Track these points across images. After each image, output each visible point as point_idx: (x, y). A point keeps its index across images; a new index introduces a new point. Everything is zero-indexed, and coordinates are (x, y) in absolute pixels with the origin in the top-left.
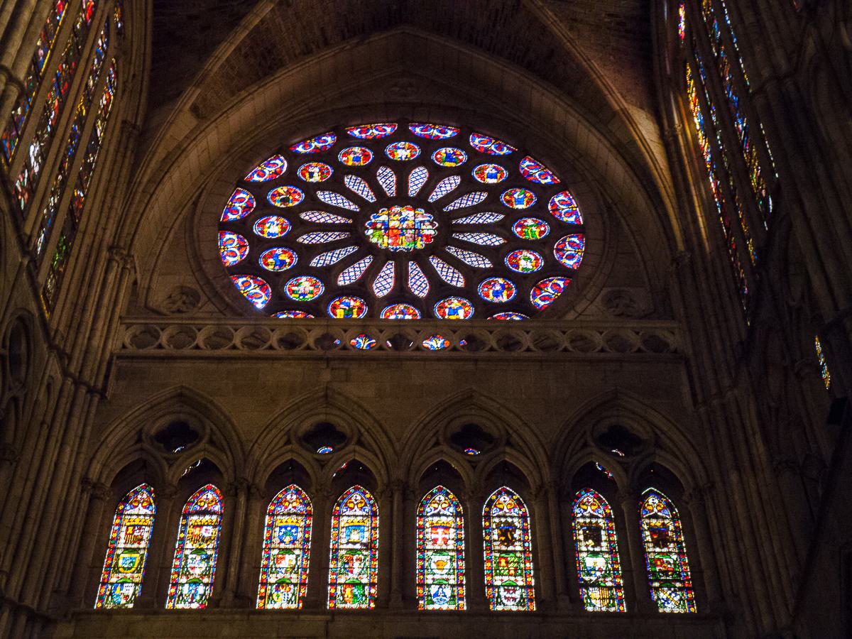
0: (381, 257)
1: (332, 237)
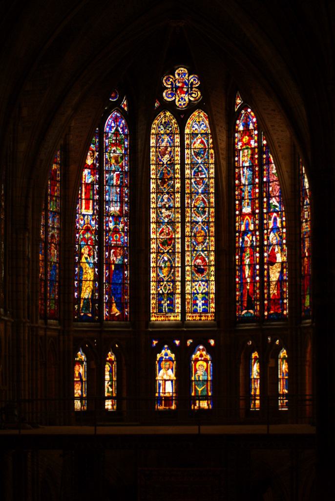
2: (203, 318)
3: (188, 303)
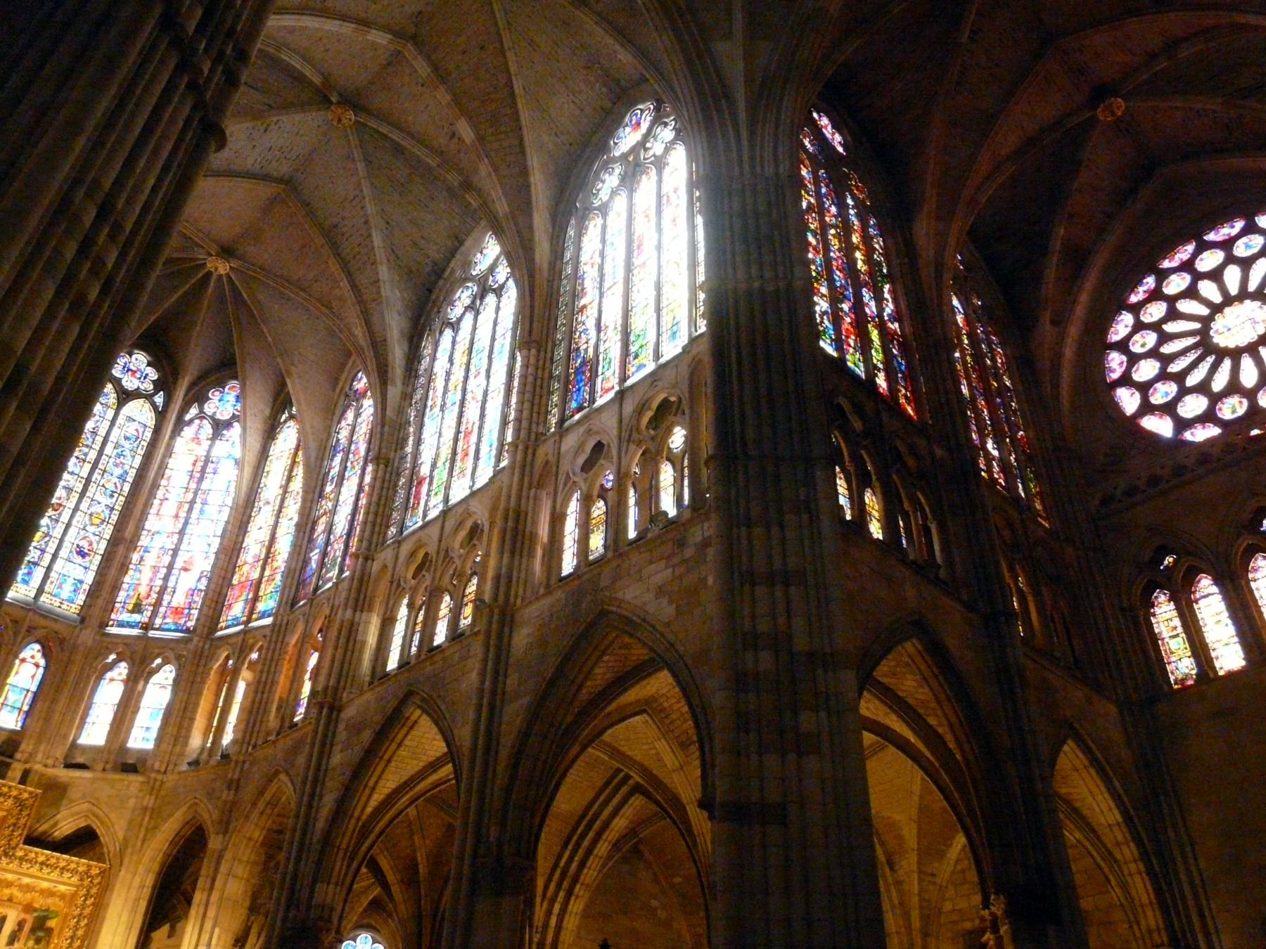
0: (1235, 354)
1: (1192, 356)
2: (63, 606)
3: (52, 583)
